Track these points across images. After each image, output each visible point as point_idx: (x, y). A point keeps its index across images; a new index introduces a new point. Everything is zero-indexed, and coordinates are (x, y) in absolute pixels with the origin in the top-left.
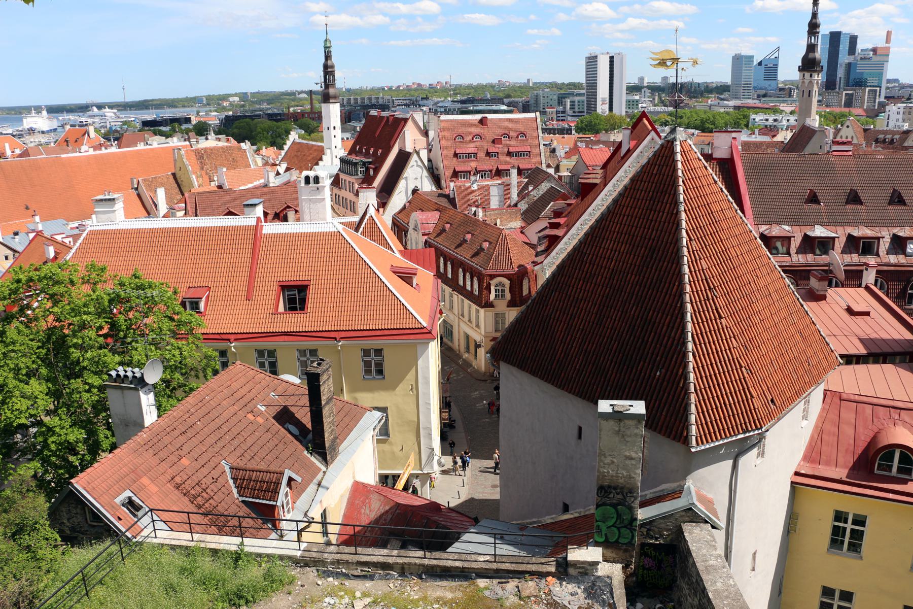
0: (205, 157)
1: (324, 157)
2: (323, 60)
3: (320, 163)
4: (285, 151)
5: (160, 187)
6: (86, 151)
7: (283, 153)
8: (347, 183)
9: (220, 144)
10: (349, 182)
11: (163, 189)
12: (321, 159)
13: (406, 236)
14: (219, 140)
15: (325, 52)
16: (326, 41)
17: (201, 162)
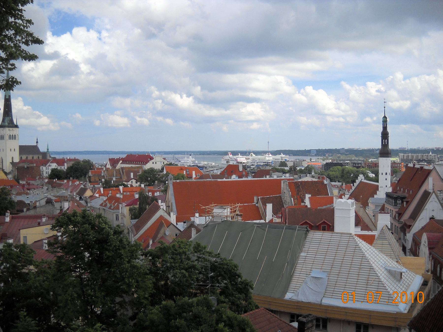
0: (300, 187)
1: (378, 192)
2: (381, 129)
3: (375, 196)
4: (355, 187)
5: (269, 203)
6: (234, 178)
7: (353, 188)
8: (389, 210)
9: (314, 180)
10: (390, 210)
11: (271, 205)
12: (376, 193)
13: (419, 249)
14: (313, 177)
15: (383, 125)
16: (385, 117)
17: (298, 190)
